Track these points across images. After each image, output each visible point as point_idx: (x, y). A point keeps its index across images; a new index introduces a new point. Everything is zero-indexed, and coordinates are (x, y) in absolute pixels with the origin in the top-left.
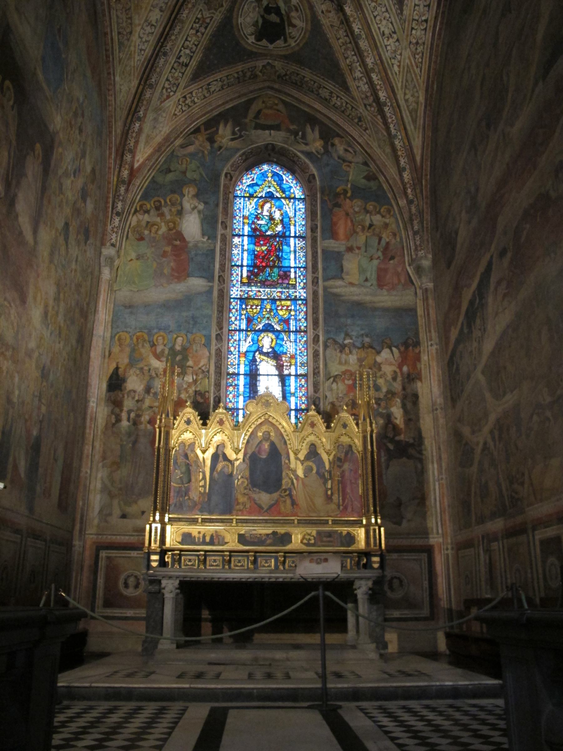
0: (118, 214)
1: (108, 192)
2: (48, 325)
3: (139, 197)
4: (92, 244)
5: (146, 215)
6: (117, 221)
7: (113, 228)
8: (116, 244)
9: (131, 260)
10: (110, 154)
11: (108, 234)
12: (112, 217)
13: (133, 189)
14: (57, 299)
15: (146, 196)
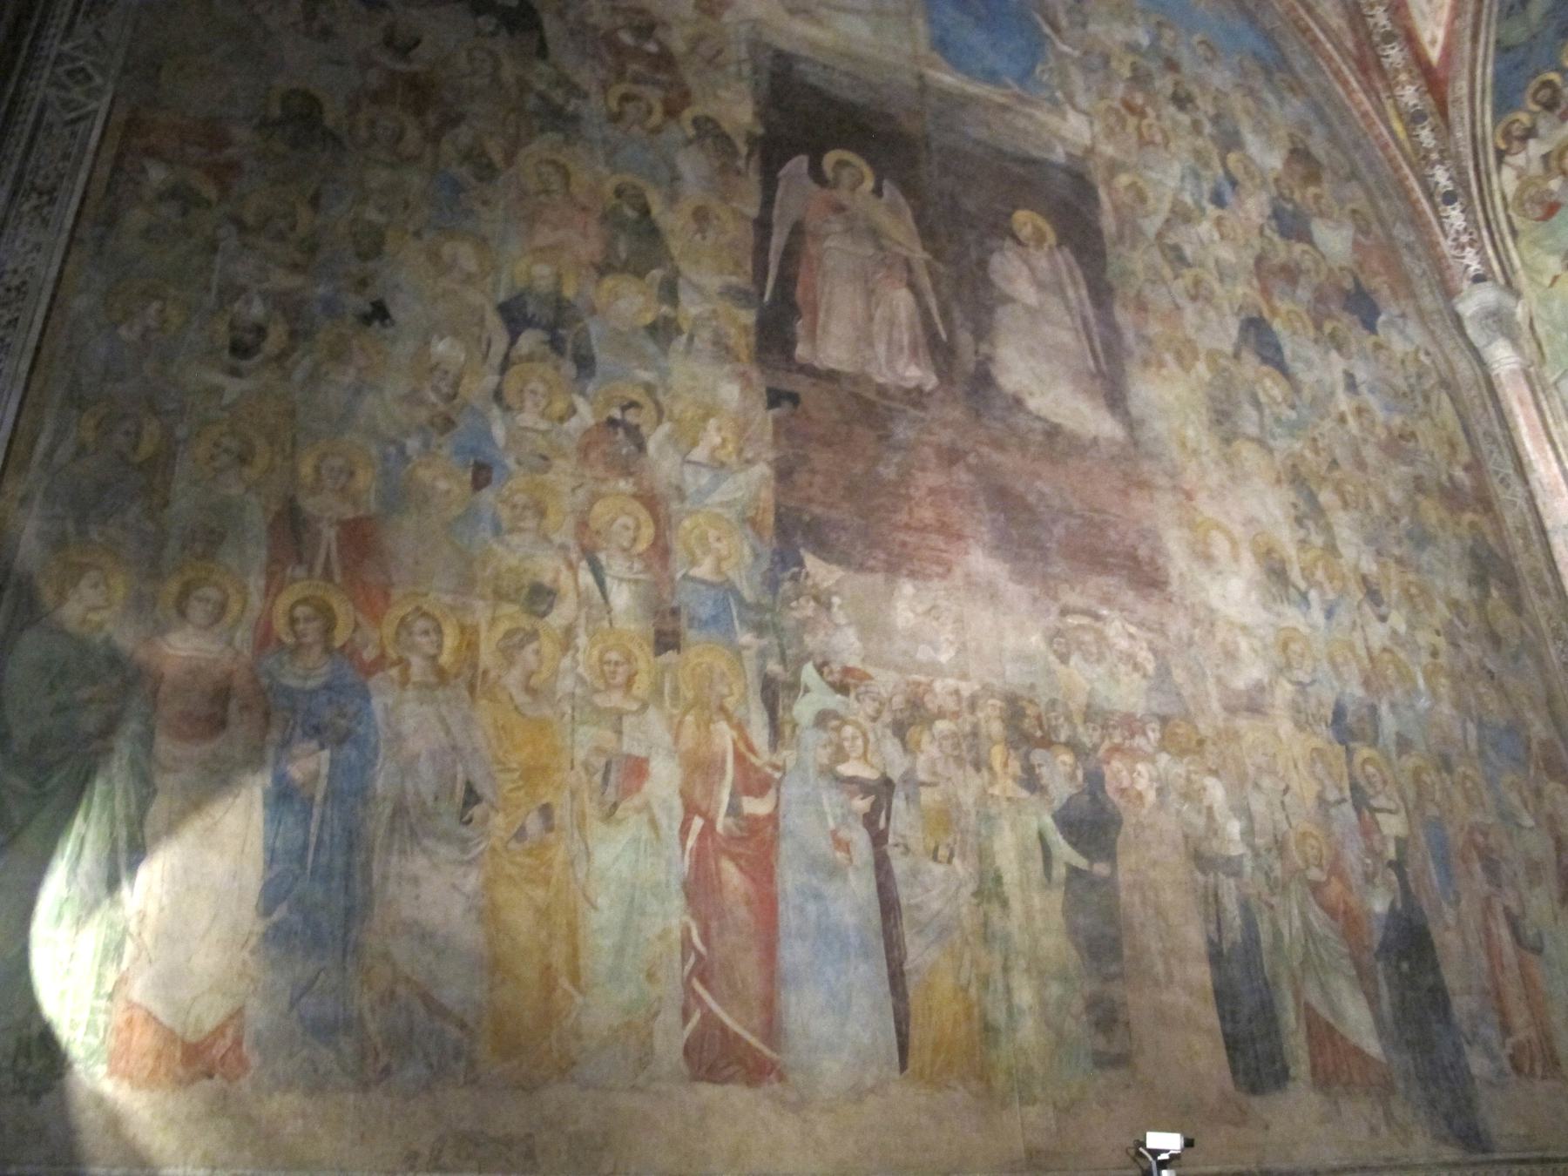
0: (1450, 198)
1: (1397, 169)
2: (1304, 596)
3: (1488, 120)
4: (1403, 315)
5: (1532, 143)
6: (1455, 217)
7: (1455, 240)
8: (1493, 272)
9: (1555, 279)
10: (1345, 83)
11: (1451, 261)
12: (1439, 218)
13: (1460, 113)
14: (1309, 513)
15: (1505, 102)
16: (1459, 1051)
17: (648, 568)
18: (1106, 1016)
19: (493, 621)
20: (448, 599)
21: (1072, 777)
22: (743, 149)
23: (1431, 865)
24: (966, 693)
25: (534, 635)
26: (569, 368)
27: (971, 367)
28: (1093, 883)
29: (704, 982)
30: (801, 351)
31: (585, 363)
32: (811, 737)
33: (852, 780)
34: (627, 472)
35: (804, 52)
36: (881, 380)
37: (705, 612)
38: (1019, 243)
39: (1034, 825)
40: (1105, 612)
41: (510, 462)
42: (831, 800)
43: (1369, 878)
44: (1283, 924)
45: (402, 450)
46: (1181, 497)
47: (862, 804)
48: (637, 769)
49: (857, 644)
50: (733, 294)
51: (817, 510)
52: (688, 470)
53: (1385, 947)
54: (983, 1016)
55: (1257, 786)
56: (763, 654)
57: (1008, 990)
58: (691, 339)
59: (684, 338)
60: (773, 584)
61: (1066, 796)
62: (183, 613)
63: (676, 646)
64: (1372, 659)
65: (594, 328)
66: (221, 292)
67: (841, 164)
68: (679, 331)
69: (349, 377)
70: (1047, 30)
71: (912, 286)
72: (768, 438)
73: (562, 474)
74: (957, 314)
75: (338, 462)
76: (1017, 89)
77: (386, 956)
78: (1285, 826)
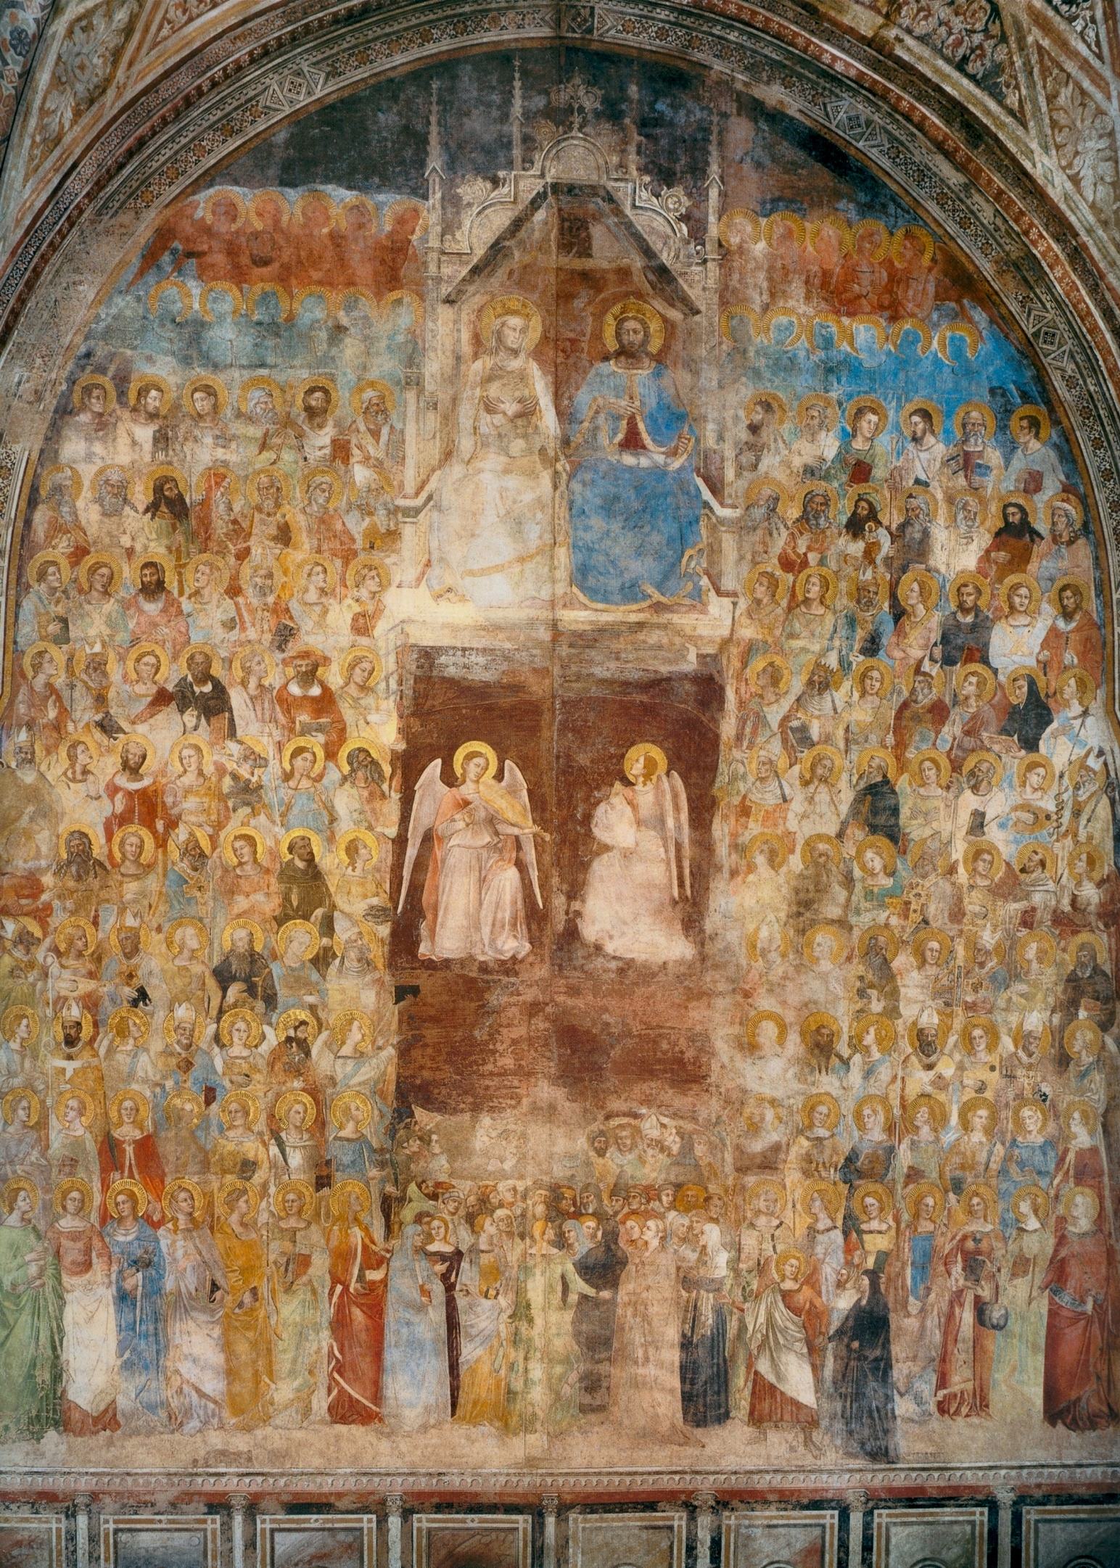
16: (889, 1399)
17: (312, 1137)
18: (592, 1384)
19: (220, 1189)
20: (196, 1179)
21: (594, 1236)
22: (387, 769)
23: (909, 1271)
24: (520, 1189)
25: (245, 1192)
26: (260, 1005)
27: (560, 927)
28: (597, 1303)
29: (341, 1375)
30: (424, 949)
31: (270, 1000)
32: (410, 1230)
33: (435, 1254)
34: (299, 1073)
35: (445, 641)
36: (482, 958)
37: (346, 1159)
38: (628, 783)
39: (559, 1270)
40: (644, 1111)
41: (227, 1084)
42: (421, 1266)
43: (840, 1285)
44: (749, 1321)
45: (163, 1087)
46: (739, 998)
47: (440, 1268)
48: (305, 1261)
49: (447, 1165)
50: (376, 914)
51: (426, 1074)
52: (340, 1061)
53: (840, 1332)
54: (508, 1385)
55: (752, 1225)
56: (383, 1181)
57: (526, 1370)
58: (342, 962)
59: (337, 961)
60: (392, 1132)
61: (584, 1251)
62: (64, 1208)
63: (329, 1185)
64: (903, 1107)
65: (276, 969)
66: (55, 1003)
67: (470, 756)
68: (334, 956)
69: (130, 1046)
70: (707, 495)
71: (521, 866)
72: (394, 1026)
73: (258, 1085)
74: (555, 881)
75: (128, 1104)
76: (657, 596)
77: (177, 1372)
78: (771, 1252)
